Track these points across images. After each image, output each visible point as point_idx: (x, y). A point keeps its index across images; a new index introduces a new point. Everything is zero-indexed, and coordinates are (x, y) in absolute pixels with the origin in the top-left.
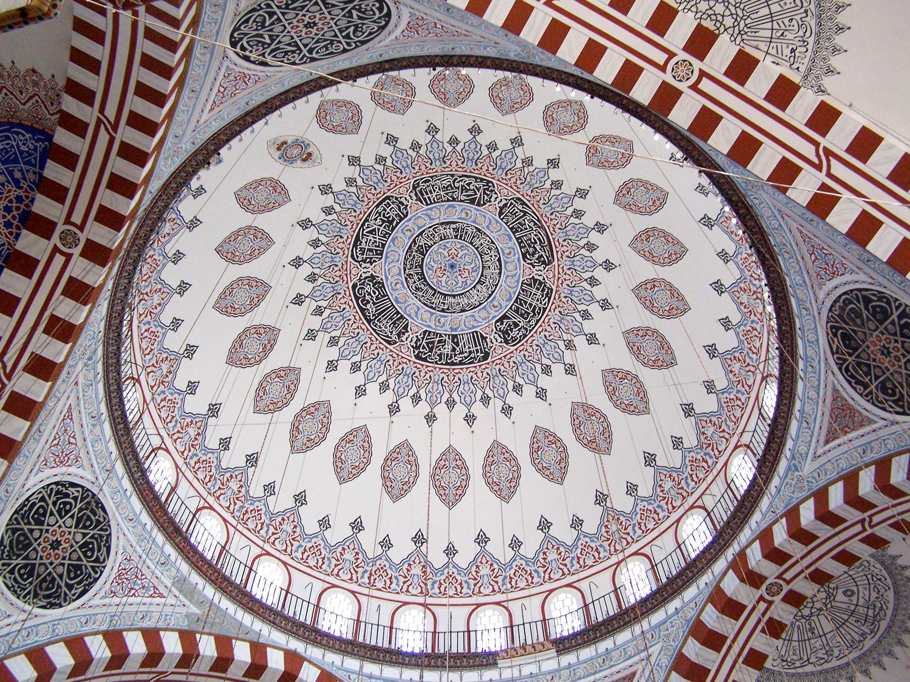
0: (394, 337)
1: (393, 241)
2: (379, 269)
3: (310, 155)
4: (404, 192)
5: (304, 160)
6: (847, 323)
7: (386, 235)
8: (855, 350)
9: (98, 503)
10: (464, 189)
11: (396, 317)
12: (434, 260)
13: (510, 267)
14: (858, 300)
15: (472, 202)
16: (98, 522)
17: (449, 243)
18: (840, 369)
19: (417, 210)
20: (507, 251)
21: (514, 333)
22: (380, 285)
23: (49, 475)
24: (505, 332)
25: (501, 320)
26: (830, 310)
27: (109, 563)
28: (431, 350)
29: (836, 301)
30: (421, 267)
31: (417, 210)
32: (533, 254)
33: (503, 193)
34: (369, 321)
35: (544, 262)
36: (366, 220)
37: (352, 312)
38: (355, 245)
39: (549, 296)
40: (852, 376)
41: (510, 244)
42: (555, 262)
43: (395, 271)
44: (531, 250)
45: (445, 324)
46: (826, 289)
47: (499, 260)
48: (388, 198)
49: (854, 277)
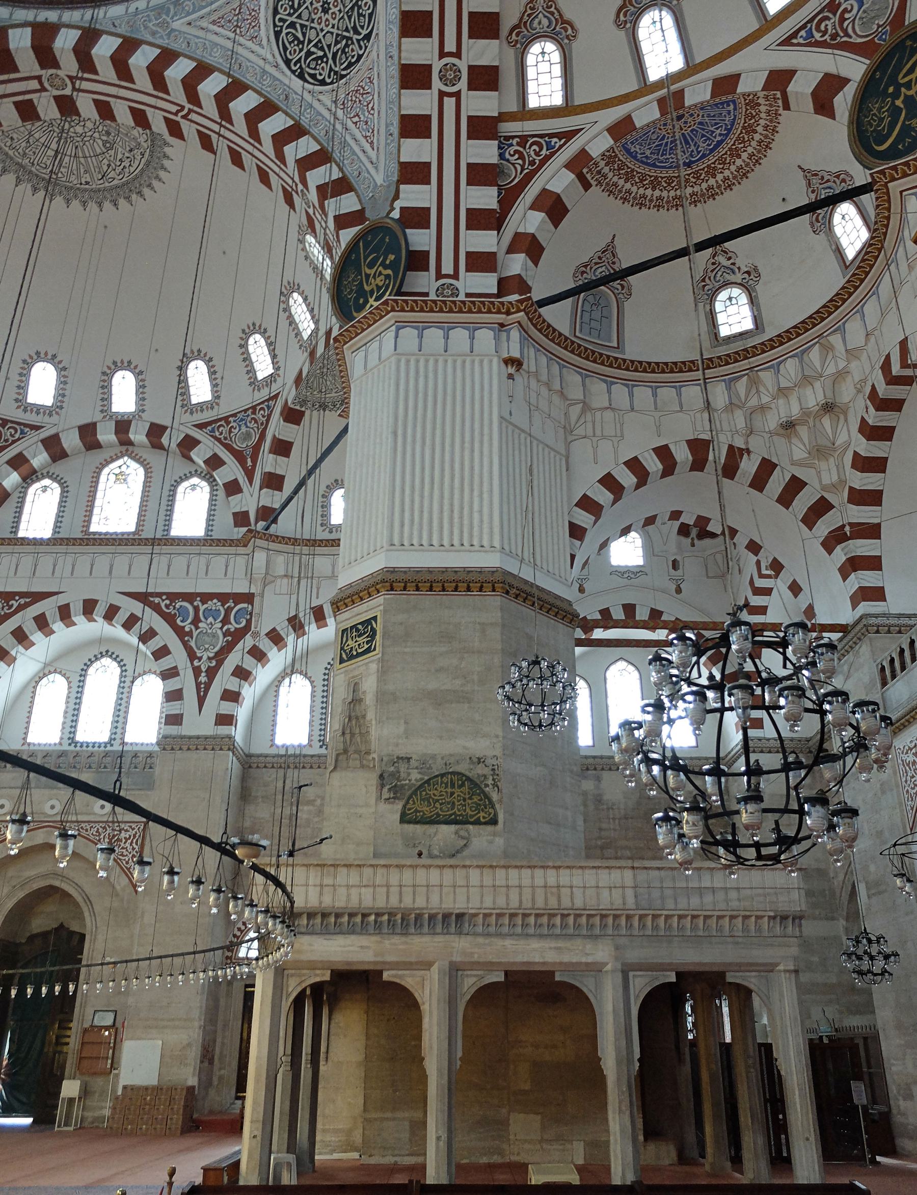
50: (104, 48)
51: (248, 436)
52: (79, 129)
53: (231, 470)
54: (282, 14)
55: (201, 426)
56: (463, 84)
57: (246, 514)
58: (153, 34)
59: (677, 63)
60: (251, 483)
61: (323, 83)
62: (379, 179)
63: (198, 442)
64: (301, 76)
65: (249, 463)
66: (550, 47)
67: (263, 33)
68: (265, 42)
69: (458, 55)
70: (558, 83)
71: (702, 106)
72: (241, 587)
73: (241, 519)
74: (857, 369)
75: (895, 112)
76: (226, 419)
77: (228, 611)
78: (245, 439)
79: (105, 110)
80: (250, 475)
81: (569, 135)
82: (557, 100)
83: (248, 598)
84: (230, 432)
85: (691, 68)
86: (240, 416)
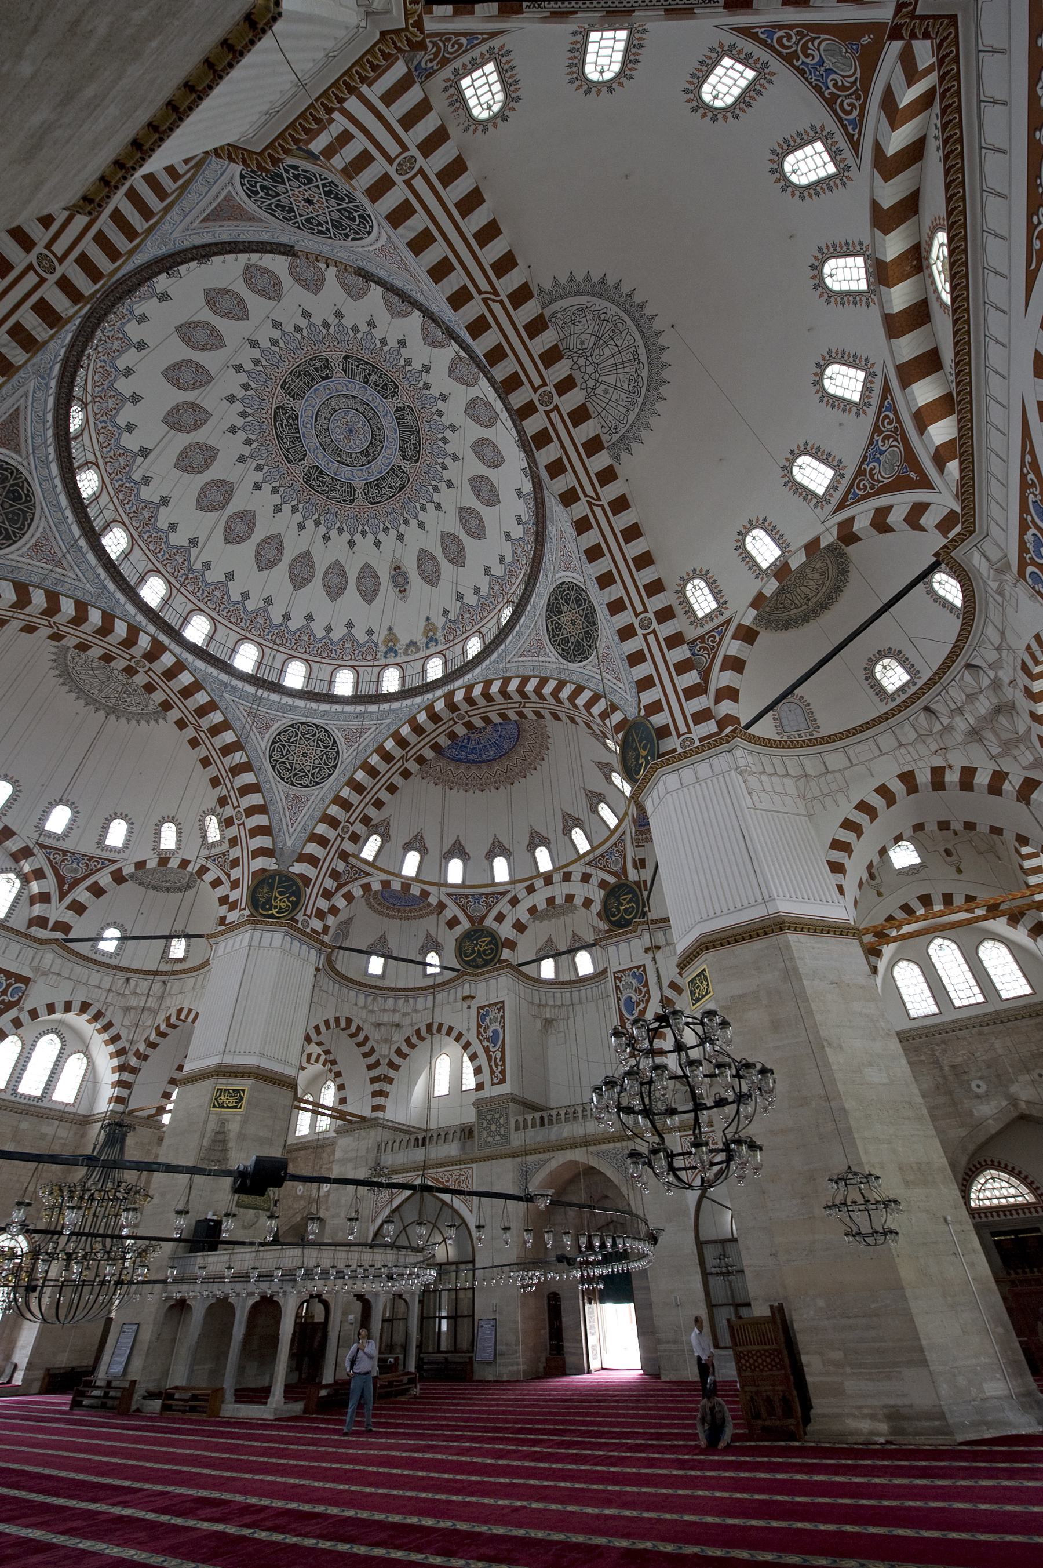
0: (407, 410)
1: (381, 473)
2: (397, 460)
3: (395, 569)
4: (361, 501)
5: (399, 568)
6: (19, 509)
7: (383, 478)
8: (9, 491)
9: (548, 605)
10: (323, 483)
11: (401, 421)
12: (360, 442)
13: (309, 413)
14: (14, 533)
15: (321, 472)
16: (556, 599)
17: (347, 449)
18: (17, 470)
19: (359, 484)
20: (309, 426)
21: (319, 364)
22: (402, 449)
23: (549, 648)
24: (326, 367)
25: (327, 377)
26: (34, 514)
27: (567, 580)
28: (386, 384)
29: (29, 525)
30: (371, 443)
31: (359, 484)
32: (290, 417)
33: (298, 471)
34: (418, 432)
35: (283, 409)
36: (390, 497)
37: (425, 448)
38: (404, 486)
39: (285, 383)
40: (6, 470)
41: (304, 430)
42: (274, 407)
43: (389, 451)
44: (290, 421)
45: (369, 394)
46: (41, 530)
47: (316, 421)
48: (372, 504)
49: (20, 552)
50: (185, 679)
51: (75, 871)
52: (121, 678)
53: (50, 884)
54: (282, 737)
55: (43, 846)
56: (347, 836)
57: (47, 920)
58: (212, 690)
59: (413, 874)
60: (61, 900)
61: (282, 779)
62: (289, 843)
63: (33, 855)
64: (273, 767)
65: (66, 887)
66: (379, 839)
67: (267, 736)
68: (266, 739)
69: (352, 824)
70: (374, 853)
71: (414, 895)
72: (26, 972)
73: (41, 922)
74: (416, 1017)
75: (473, 952)
76: (65, 853)
77: (9, 986)
78: (71, 872)
79: (150, 688)
80: (62, 896)
81: (368, 874)
82: (371, 859)
83: (26, 981)
84: (63, 861)
85: (416, 879)
86: (78, 856)
